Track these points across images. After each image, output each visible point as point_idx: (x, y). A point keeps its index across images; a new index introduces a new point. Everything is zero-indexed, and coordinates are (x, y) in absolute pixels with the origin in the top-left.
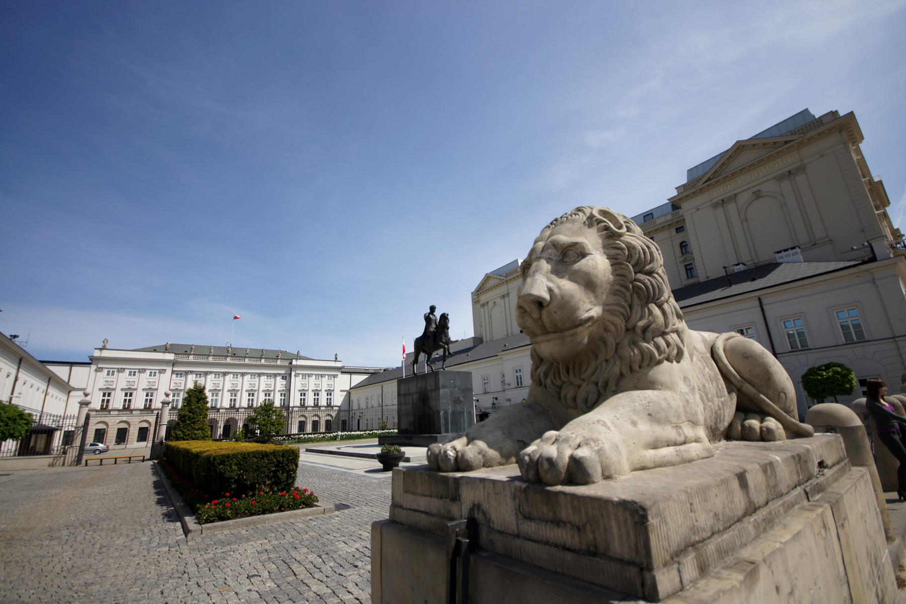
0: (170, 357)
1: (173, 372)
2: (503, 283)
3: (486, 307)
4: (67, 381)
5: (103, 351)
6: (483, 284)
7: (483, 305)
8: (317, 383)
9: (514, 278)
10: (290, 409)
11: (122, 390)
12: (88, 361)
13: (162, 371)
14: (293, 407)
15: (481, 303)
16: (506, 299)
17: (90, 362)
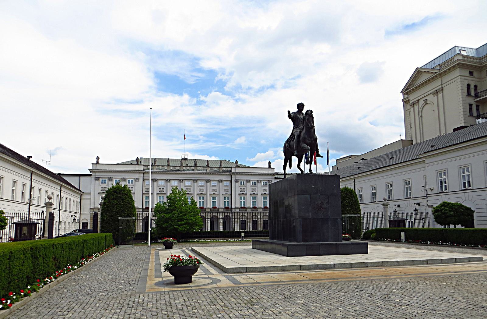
0: (141, 168)
1: (144, 179)
2: (436, 76)
3: (416, 107)
4: (78, 188)
5: (98, 165)
6: (413, 81)
7: (413, 104)
8: (254, 188)
9: (449, 69)
10: (233, 210)
12: (89, 173)
13: (137, 180)
14: (235, 208)
15: (411, 102)
16: (440, 95)
17: (91, 173)
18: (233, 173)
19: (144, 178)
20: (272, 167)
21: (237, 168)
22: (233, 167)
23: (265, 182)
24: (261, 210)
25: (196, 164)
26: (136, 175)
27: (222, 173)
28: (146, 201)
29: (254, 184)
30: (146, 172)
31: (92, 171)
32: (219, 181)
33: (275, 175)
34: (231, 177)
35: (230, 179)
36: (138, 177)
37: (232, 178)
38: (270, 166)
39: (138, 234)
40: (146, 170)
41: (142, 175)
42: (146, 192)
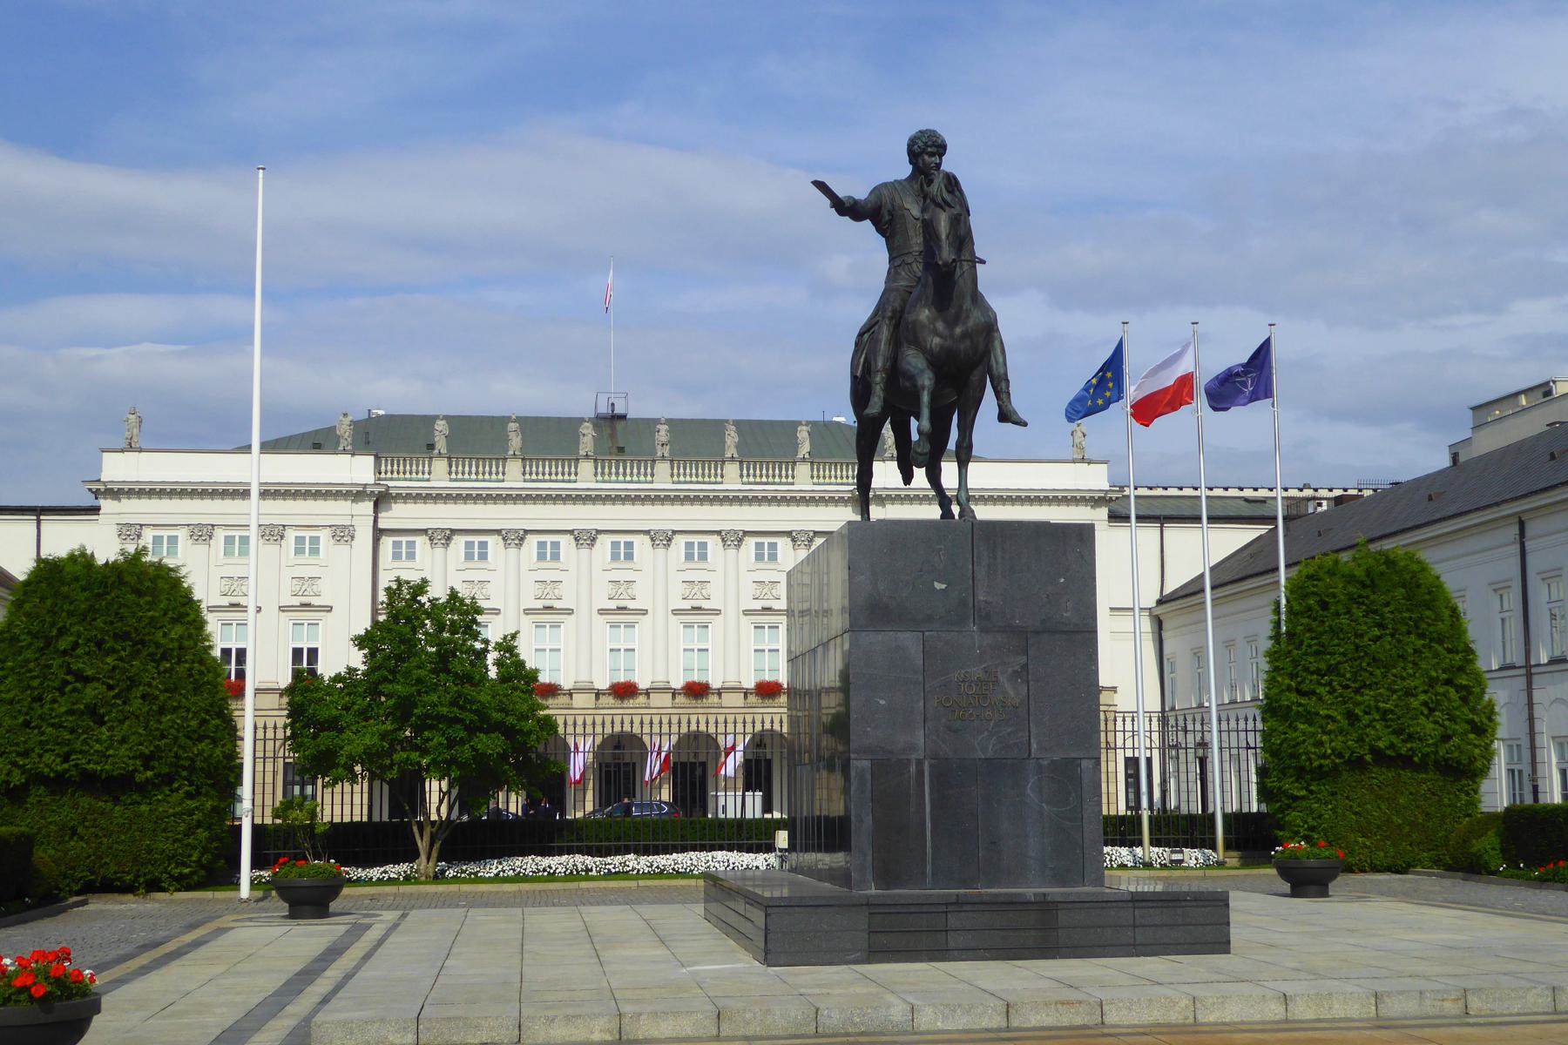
1: (378, 533)
12: (89, 501)
13: (344, 534)
19: (381, 525)
31: (102, 488)
40: (392, 479)
41: (368, 506)
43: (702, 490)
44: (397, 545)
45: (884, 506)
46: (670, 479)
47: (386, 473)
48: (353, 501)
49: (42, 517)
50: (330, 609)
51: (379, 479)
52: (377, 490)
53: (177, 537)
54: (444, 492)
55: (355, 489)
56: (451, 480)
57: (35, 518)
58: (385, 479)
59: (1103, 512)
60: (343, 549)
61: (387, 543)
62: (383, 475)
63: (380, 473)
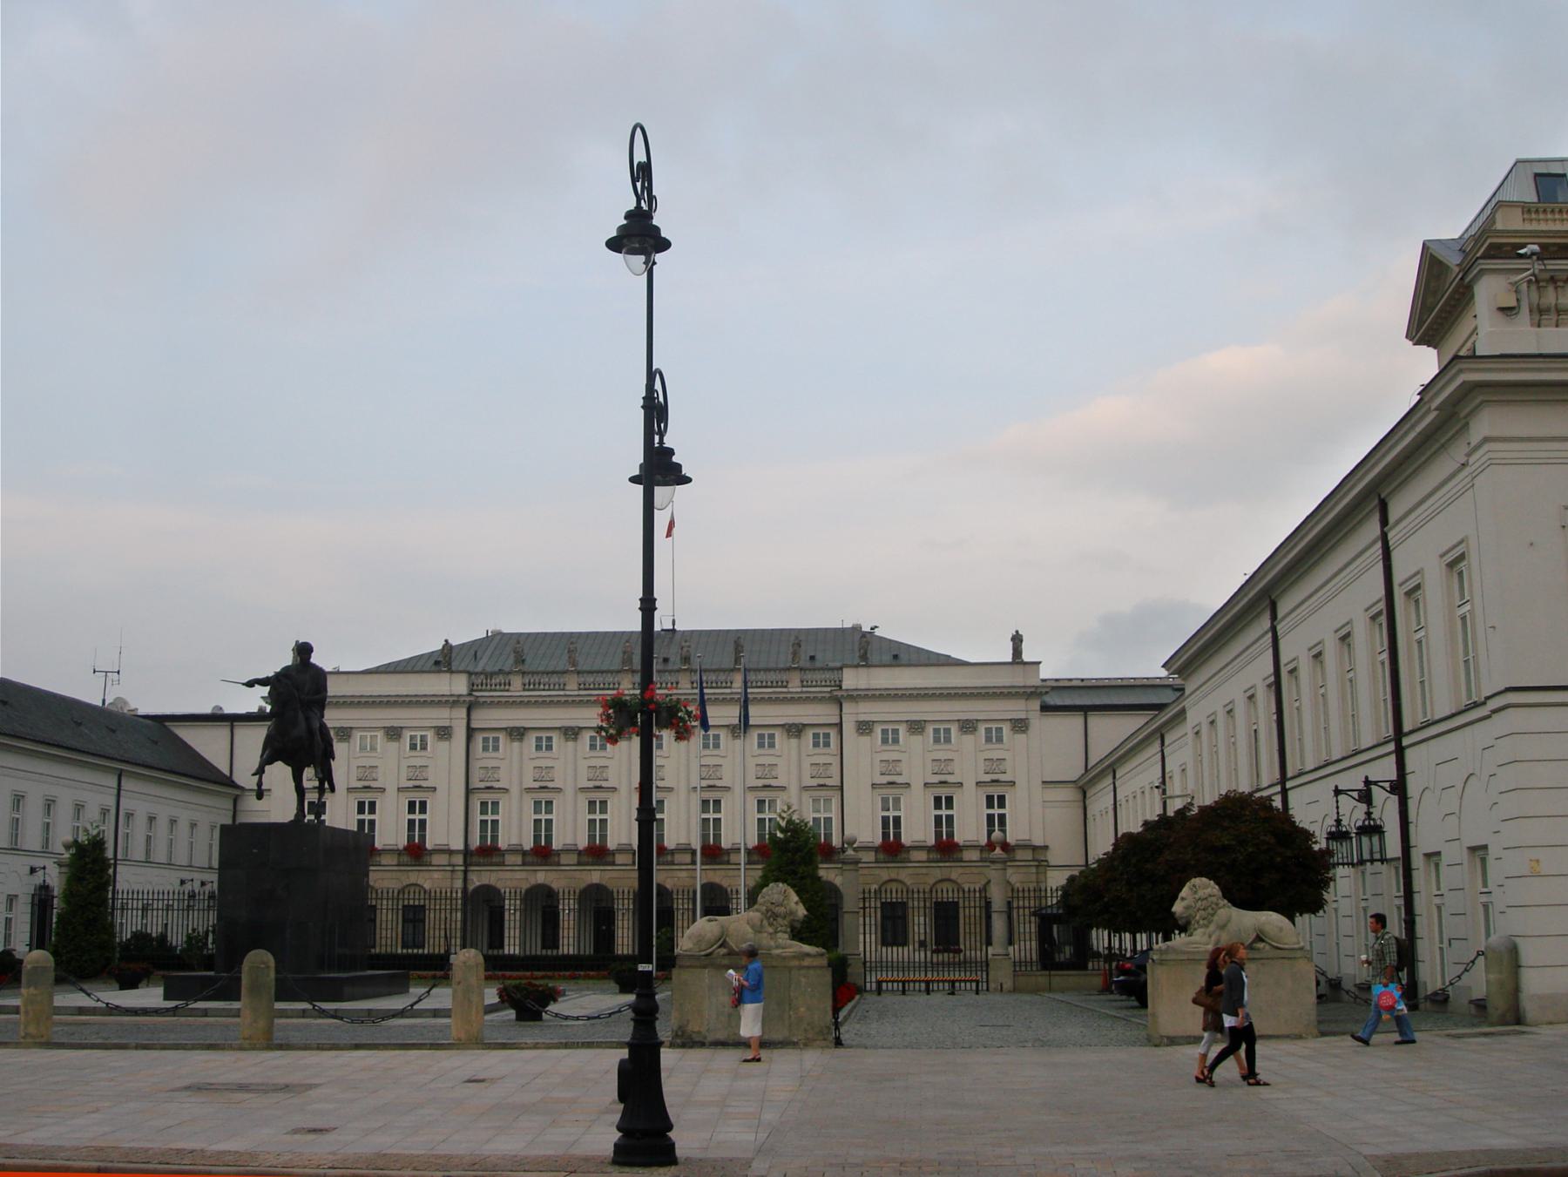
1: (470, 732)
4: (226, 771)
11: (350, 790)
13: (444, 733)
18: (845, 694)
19: (474, 725)
20: (1026, 657)
21: (863, 672)
22: (847, 667)
23: (942, 727)
24: (974, 855)
25: (686, 660)
26: (441, 716)
27: (796, 696)
28: (481, 821)
29: (942, 737)
30: (482, 700)
32: (788, 731)
33: (1041, 694)
34: (841, 710)
35: (836, 720)
36: (447, 724)
37: (843, 716)
38: (1017, 652)
39: (512, 957)
40: (481, 690)
41: (463, 713)
42: (483, 785)
43: (714, 694)
44: (486, 740)
45: (857, 702)
46: (689, 686)
47: (487, 685)
48: (451, 708)
49: (235, 724)
50: (434, 789)
51: (472, 690)
52: (468, 699)
53: (377, 736)
54: (519, 700)
55: (451, 699)
56: (524, 690)
57: (229, 724)
58: (476, 691)
59: (1035, 705)
60: (444, 745)
61: (479, 740)
62: (475, 687)
63: (473, 685)
